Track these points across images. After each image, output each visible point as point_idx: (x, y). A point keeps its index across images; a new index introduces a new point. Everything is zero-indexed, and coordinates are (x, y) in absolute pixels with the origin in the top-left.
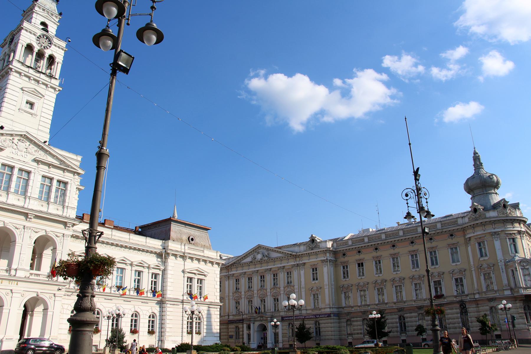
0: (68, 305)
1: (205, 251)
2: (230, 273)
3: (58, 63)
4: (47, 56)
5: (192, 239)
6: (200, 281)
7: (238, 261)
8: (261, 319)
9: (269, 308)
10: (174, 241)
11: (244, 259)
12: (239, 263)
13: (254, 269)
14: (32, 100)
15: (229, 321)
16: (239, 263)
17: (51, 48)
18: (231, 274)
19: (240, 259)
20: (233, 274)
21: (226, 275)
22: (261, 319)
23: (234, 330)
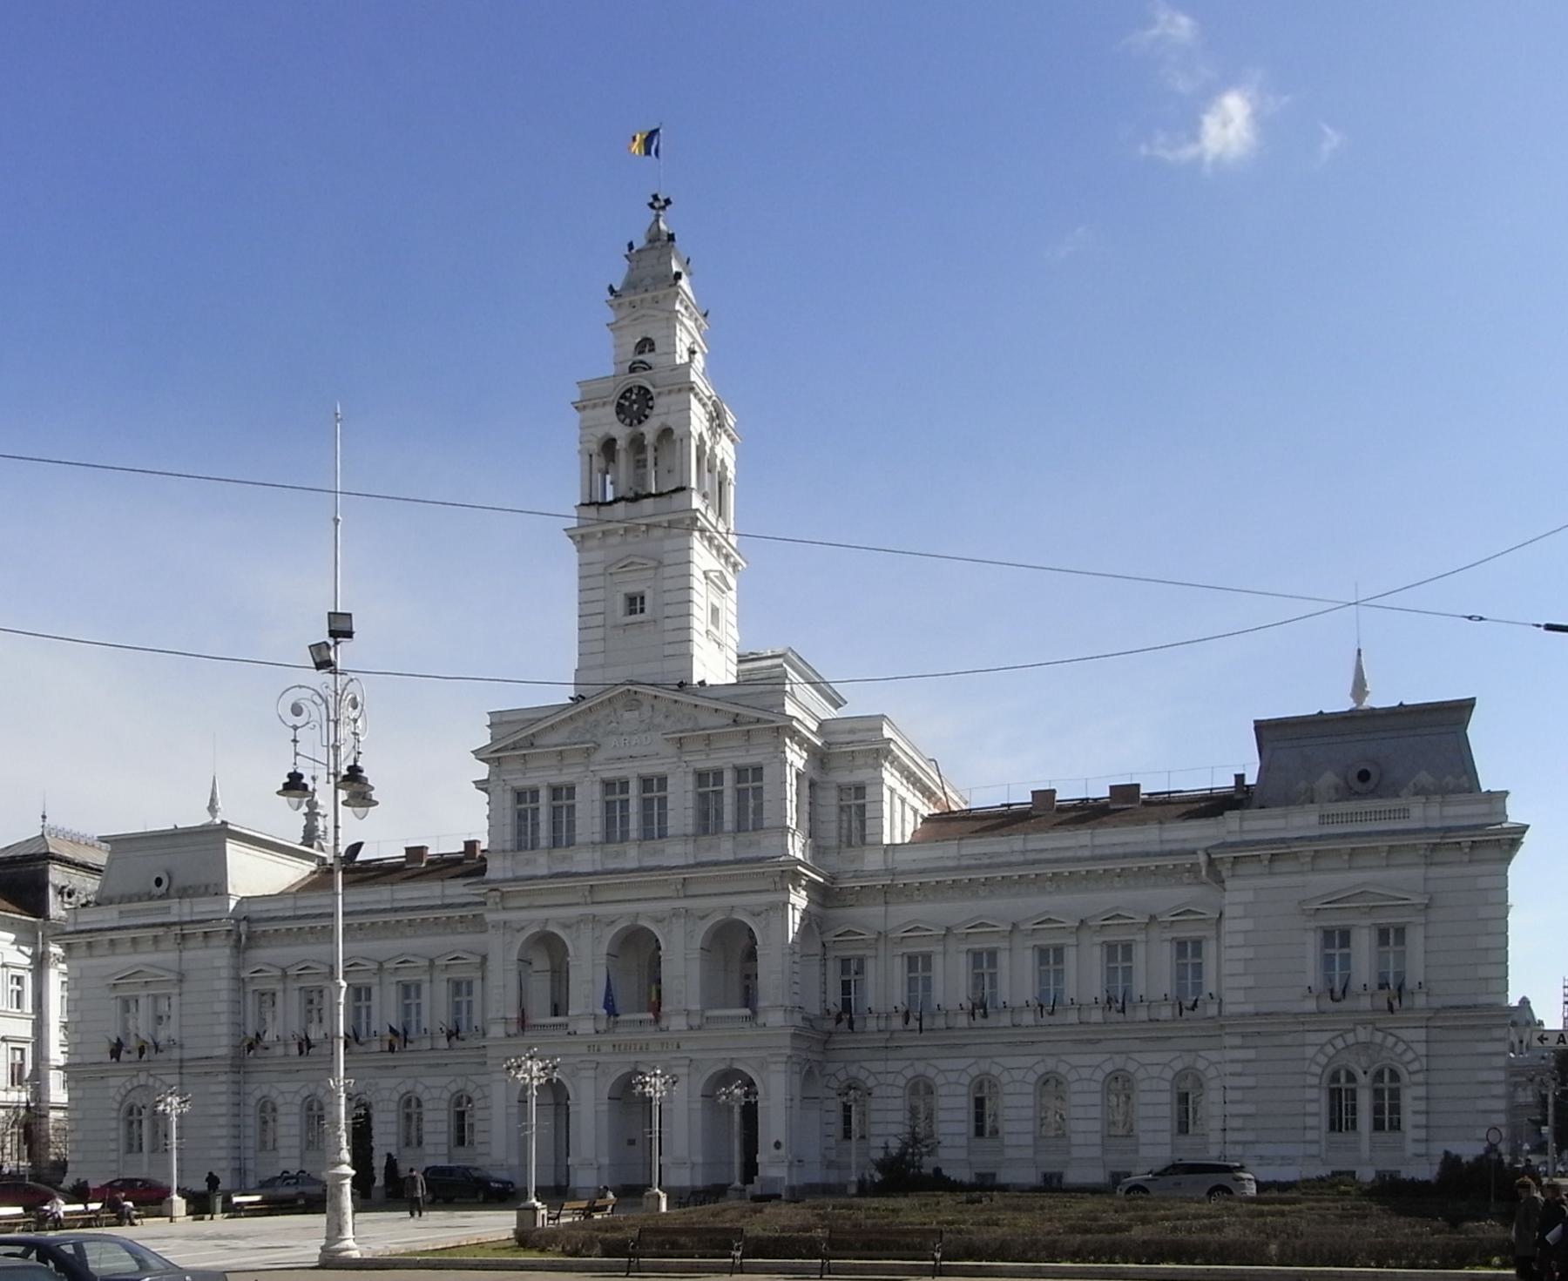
0: (1161, 1067)
3: (681, 440)
4: (650, 439)
14: (633, 589)
17: (656, 411)
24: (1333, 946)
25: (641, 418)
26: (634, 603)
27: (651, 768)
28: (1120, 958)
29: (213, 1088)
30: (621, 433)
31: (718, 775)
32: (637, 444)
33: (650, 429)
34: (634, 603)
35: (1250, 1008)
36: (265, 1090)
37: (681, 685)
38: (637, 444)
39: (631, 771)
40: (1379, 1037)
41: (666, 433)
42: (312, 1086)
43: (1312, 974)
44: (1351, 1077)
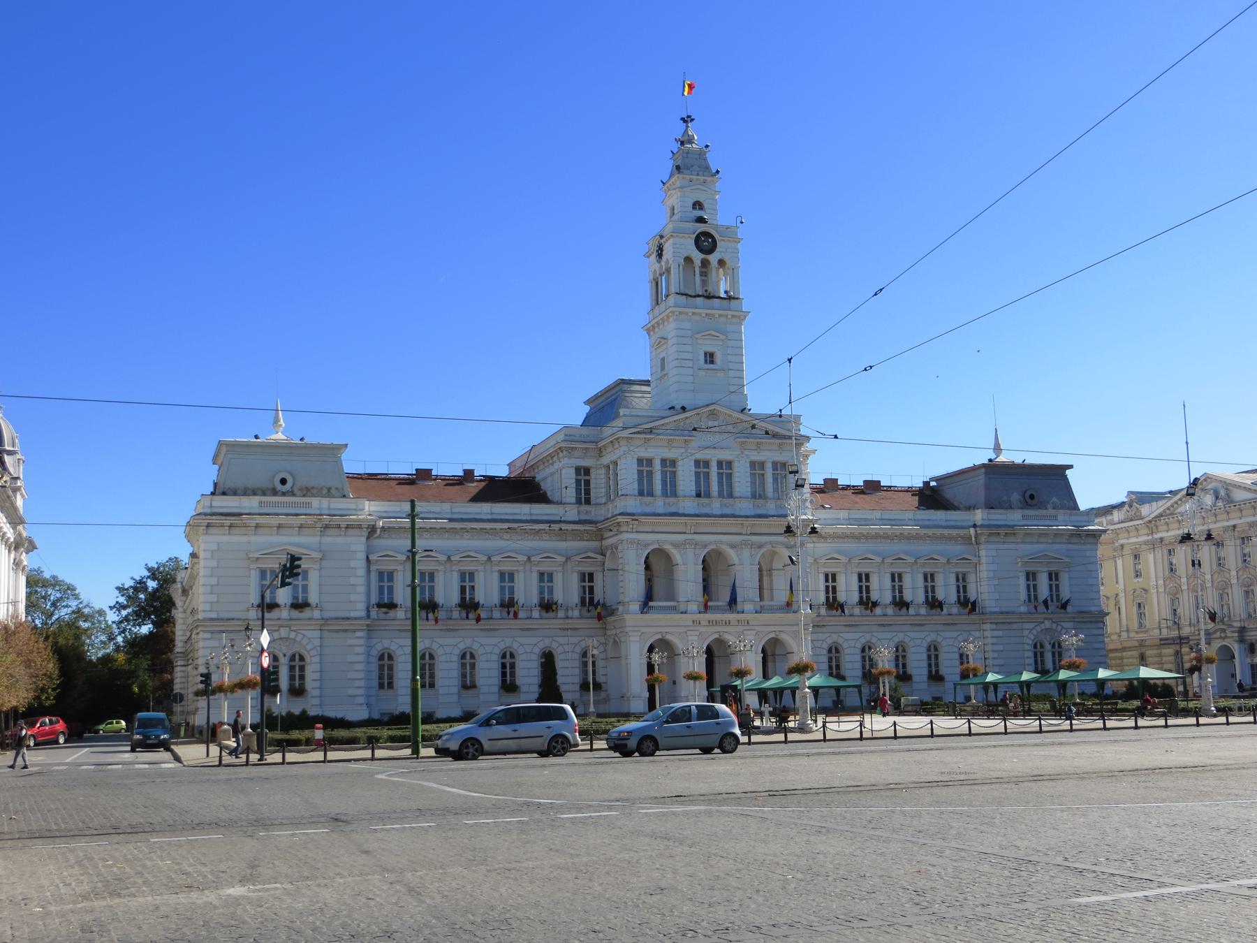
1: (1061, 517)
2: (1155, 536)
5: (1032, 497)
6: (1053, 576)
7: (1168, 509)
8: (1223, 635)
9: (1237, 612)
10: (992, 508)
11: (1181, 505)
12: (1171, 514)
13: (1226, 524)
14: (710, 349)
15: (1161, 640)
16: (1171, 514)
18: (1156, 539)
19: (1172, 506)
20: (1162, 539)
21: (1148, 541)
22: (1223, 635)
23: (1172, 659)
24: (505, 582)
25: (711, 250)
26: (710, 358)
27: (725, 455)
28: (507, 580)
29: (350, 642)
30: (697, 257)
31: (762, 464)
32: (705, 264)
33: (713, 258)
34: (710, 358)
35: (997, 609)
36: (386, 643)
37: (743, 410)
38: (705, 264)
39: (714, 456)
40: (1054, 626)
41: (721, 263)
42: (868, 636)
43: (1023, 595)
44: (1042, 646)
